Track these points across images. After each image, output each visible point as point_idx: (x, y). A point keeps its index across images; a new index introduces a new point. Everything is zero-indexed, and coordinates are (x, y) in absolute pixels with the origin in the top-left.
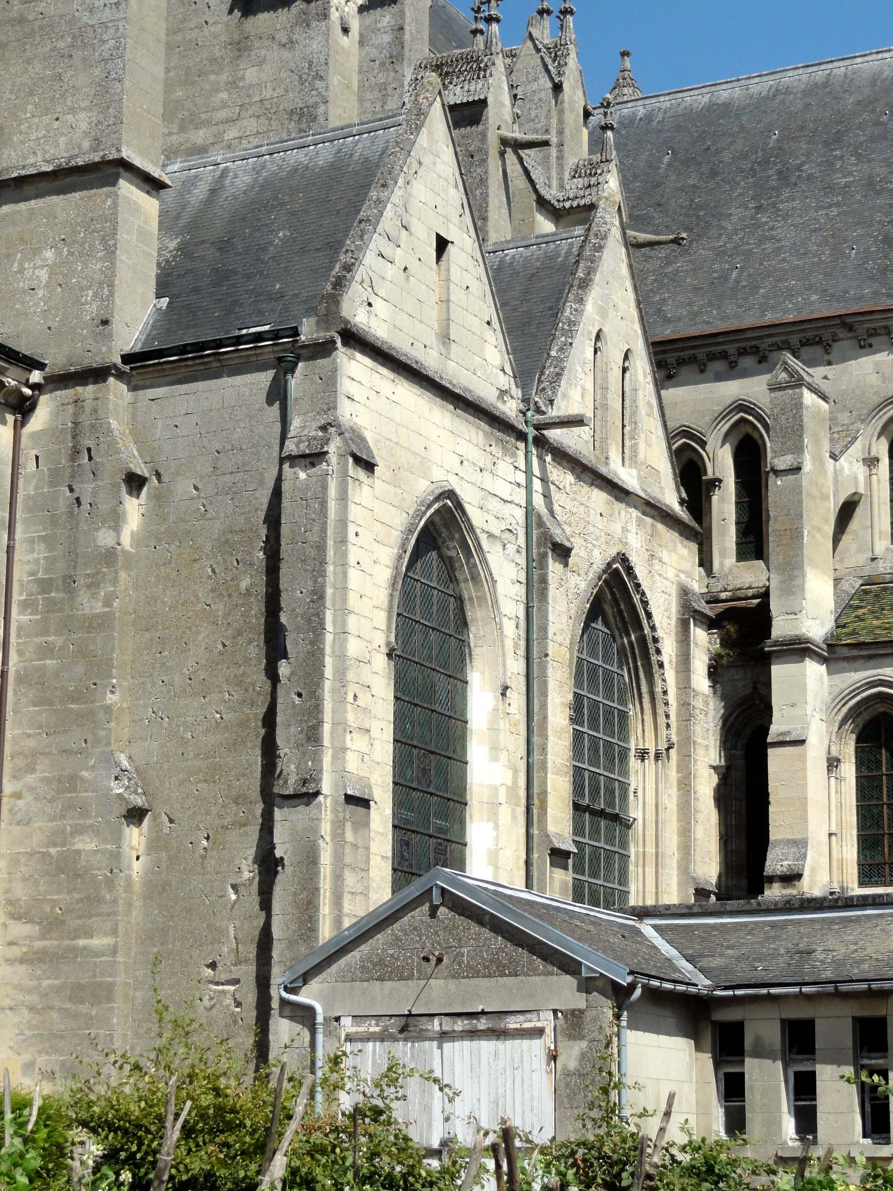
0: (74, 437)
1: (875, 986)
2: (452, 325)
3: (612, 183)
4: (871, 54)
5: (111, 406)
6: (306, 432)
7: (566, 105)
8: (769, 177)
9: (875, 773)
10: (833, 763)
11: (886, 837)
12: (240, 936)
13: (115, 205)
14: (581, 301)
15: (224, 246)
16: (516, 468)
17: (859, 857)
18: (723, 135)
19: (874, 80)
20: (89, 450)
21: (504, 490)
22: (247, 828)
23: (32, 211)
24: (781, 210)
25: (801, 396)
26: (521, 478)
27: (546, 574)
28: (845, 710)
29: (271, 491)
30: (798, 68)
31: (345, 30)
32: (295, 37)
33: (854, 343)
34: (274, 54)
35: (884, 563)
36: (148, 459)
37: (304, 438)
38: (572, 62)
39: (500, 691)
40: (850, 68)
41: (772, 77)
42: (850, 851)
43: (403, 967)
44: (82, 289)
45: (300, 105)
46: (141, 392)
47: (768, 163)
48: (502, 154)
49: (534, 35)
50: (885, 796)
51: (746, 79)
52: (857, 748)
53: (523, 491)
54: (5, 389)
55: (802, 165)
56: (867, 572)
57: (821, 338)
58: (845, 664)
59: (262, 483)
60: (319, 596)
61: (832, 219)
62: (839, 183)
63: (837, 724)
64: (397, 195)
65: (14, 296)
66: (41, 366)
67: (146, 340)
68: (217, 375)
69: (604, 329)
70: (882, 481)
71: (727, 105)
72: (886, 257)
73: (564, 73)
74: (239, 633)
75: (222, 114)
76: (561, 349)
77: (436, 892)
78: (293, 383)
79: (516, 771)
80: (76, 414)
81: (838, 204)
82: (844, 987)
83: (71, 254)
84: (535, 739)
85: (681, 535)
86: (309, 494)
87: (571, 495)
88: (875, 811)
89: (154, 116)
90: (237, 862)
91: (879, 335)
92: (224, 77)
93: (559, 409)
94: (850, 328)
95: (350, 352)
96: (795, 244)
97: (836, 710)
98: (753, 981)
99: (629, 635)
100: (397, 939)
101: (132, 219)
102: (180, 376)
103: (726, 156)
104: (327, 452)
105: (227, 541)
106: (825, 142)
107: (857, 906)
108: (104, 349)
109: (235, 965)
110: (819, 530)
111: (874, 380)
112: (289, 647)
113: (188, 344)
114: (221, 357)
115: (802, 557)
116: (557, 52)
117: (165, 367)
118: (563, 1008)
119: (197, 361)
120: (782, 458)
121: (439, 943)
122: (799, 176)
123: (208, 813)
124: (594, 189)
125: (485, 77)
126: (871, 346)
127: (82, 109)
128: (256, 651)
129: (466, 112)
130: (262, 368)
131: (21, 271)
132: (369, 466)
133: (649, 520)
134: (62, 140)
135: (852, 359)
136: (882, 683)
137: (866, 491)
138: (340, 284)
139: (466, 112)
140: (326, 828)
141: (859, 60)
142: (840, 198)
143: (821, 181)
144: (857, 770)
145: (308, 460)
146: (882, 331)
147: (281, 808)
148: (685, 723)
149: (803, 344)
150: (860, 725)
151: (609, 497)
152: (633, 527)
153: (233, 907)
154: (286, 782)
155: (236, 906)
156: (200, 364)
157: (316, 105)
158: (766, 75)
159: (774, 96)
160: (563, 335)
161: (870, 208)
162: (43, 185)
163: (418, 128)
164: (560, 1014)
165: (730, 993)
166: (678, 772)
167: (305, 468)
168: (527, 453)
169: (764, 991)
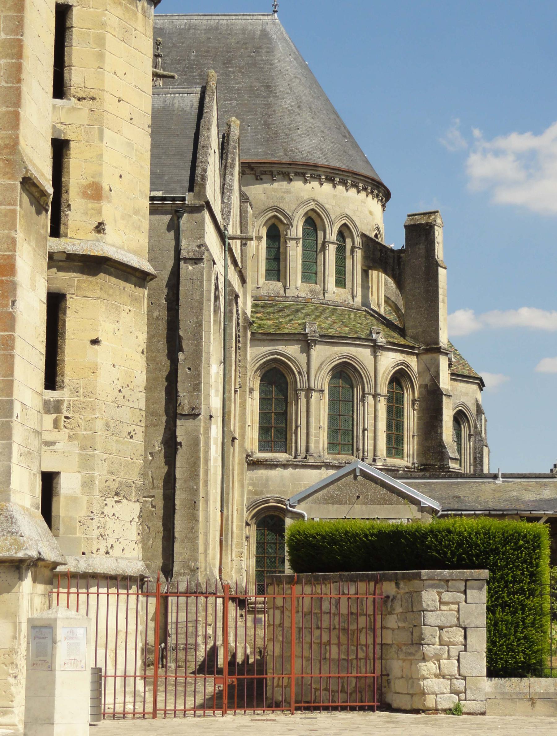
1: (505, 512)
4: (240, 15)
6: (190, 247)
8: (194, 76)
9: (269, 397)
11: (273, 428)
12: (154, 476)
19: (244, 30)
22: (158, 427)
28: (258, 365)
29: (169, 272)
30: (200, 15)
33: (254, 177)
40: (229, 21)
41: (186, 18)
43: (342, 499)
47: (192, 68)
51: (170, 16)
58: (259, 343)
59: (164, 267)
60: (199, 325)
61: (234, 107)
62: (234, 87)
63: (253, 372)
72: (267, 133)
76: (228, 199)
77: (358, 471)
82: (493, 512)
84: (227, 386)
86: (194, 277)
88: (268, 416)
90: (153, 442)
91: (267, 174)
94: (252, 169)
98: (452, 509)
100: (340, 488)
106: (222, 62)
109: (152, 489)
111: (262, 197)
112: (184, 346)
121: (358, 490)
126: (261, 179)
130: (166, 213)
135: (252, 185)
136: (277, 353)
141: (234, 17)
142: (236, 96)
143: (225, 84)
145: (193, 261)
147: (180, 419)
153: (150, 463)
154: (183, 408)
155: (152, 462)
158: (182, 16)
159: (189, 29)
161: (254, 104)
165: (446, 513)
169: (460, 513)
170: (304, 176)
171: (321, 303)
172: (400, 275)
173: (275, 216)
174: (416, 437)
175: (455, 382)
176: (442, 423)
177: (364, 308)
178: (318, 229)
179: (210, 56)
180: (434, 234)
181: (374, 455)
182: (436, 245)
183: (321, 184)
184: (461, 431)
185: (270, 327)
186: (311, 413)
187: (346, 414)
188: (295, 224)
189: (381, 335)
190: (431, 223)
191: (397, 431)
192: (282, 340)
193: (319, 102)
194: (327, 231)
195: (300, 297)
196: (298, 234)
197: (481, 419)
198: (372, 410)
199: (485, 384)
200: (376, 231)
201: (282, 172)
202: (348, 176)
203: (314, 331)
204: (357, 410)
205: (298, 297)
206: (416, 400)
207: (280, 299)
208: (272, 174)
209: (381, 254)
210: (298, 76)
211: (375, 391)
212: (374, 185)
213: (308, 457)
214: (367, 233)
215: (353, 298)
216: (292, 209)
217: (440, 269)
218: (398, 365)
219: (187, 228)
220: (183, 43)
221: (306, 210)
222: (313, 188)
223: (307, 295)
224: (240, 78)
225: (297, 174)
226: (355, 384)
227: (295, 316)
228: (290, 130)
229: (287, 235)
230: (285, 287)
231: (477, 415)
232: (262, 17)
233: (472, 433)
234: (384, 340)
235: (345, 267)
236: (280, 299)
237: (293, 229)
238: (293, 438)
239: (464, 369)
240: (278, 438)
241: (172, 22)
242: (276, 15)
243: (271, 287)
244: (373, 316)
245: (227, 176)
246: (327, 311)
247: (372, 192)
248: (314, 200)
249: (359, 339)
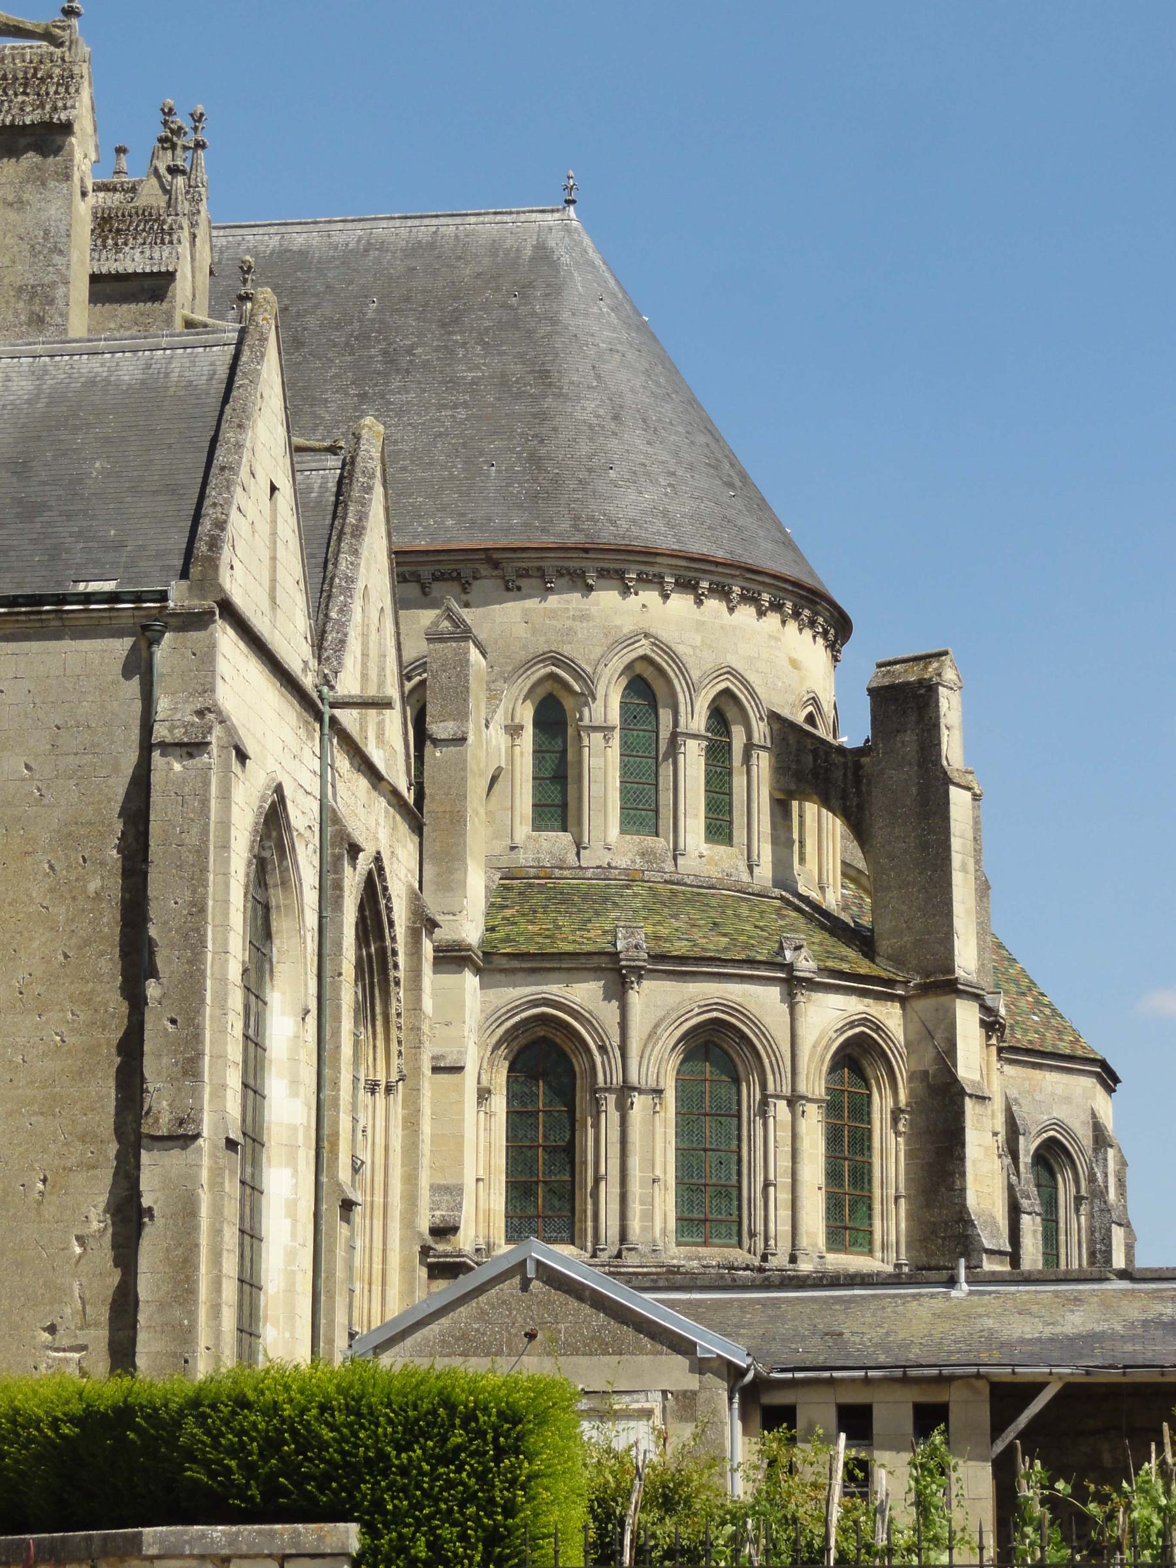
1: (946, 1371)
4: (487, 214)
6: (178, 716)
8: (371, 357)
9: (530, 1108)
10: (484, 1094)
12: (87, 1296)
14: (355, 552)
17: (506, 1208)
18: (304, 292)
19: (494, 247)
22: (97, 1172)
24: (392, 403)
25: (467, 652)
27: (342, 879)
28: (500, 1031)
29: (128, 780)
30: (394, 218)
32: (25, 197)
33: (500, 582)
35: (525, 853)
37: (178, 723)
39: (301, 1016)
40: (461, 228)
41: (361, 225)
42: (498, 1201)
43: (491, 1343)
45: (31, 282)
47: (368, 338)
50: (541, 1135)
51: (325, 222)
52: (508, 1077)
55: (413, 347)
56: (504, 862)
57: (459, 574)
58: (501, 977)
59: (116, 768)
60: (199, 909)
61: (461, 423)
62: (464, 378)
63: (490, 1049)
68: (57, 636)
70: (526, 754)
71: (303, 253)
72: (535, 480)
74: (87, 943)
76: (341, 611)
79: (310, 1108)
81: (465, 405)
82: (913, 1372)
84: (327, 1071)
85: (410, 828)
90: (84, 1209)
91: (529, 576)
94: (496, 565)
96: (415, 449)
97: (489, 1032)
98: (808, 1364)
99: (368, 946)
100: (483, 1312)
102: (7, 632)
103: (312, 322)
104: (209, 743)
105: (70, 834)
106: (439, 321)
107: (844, 1285)
109: (81, 1329)
110: (477, 814)
111: (521, 630)
112: (160, 965)
114: (65, 616)
115: (465, 846)
118: (673, 1389)
119: (32, 617)
120: (441, 725)
121: (532, 1318)
122: (411, 361)
123: (45, 1150)
125: (171, 242)
126: (519, 589)
128: (109, 965)
129: (147, 283)
130: (119, 633)
133: (391, 810)
137: (507, 764)
139: (147, 283)
140: (204, 1175)
141: (473, 219)
142: (467, 397)
143: (441, 372)
144: (508, 1103)
145: (185, 750)
146: (536, 574)
147: (149, 1150)
148: (413, 1051)
149: (435, 579)
150: (515, 1052)
152: (382, 821)
153: (78, 1262)
154: (157, 1121)
155: (83, 1261)
156: (35, 620)
157: (53, 285)
158: (353, 221)
159: (366, 250)
161: (507, 415)
164: (669, 1396)
165: (790, 1375)
166: (403, 1108)
167: (180, 759)
169: (827, 1374)
170: (622, 579)
171: (666, 882)
172: (860, 807)
173: (552, 676)
174: (902, 1201)
175: (1038, 1072)
176: (963, 1165)
177: (777, 892)
178: (660, 705)
179: (411, 309)
180: (937, 706)
181: (794, 1245)
182: (944, 732)
183: (666, 597)
184: (1056, 1188)
185: (531, 939)
186: (630, 1147)
187: (723, 1147)
188: (600, 692)
189: (804, 952)
190: (930, 679)
191: (855, 1188)
192: (559, 969)
193: (668, 406)
194: (682, 708)
195: (616, 868)
196: (609, 717)
197: (1106, 1160)
198: (785, 1135)
199: (1119, 1074)
200: (810, 708)
201: (567, 569)
202: (733, 576)
203: (636, 947)
204: (749, 1136)
205: (610, 866)
206: (902, 1111)
207: (566, 873)
208: (543, 576)
209: (815, 760)
210: (619, 347)
211: (793, 1090)
212: (802, 597)
213: (624, 1253)
214: (786, 713)
215: (750, 868)
216: (592, 657)
217: (953, 790)
218: (852, 1025)
219: (172, 668)
220: (351, 282)
221: (627, 660)
222: (644, 606)
223: (633, 862)
224: (478, 355)
225: (603, 574)
226: (742, 1073)
227: (597, 914)
228: (590, 470)
229: (581, 719)
230: (579, 846)
231: (1095, 1150)
232: (539, 216)
233: (1083, 1193)
234: (812, 965)
235: (730, 794)
236: (566, 873)
237: (597, 707)
238: (589, 1207)
239: (1061, 1040)
240: (552, 1208)
241: (329, 236)
242: (571, 210)
243: (545, 844)
244: (798, 909)
245: (342, 556)
246: (681, 897)
247: (796, 615)
248: (646, 636)
249: (751, 962)
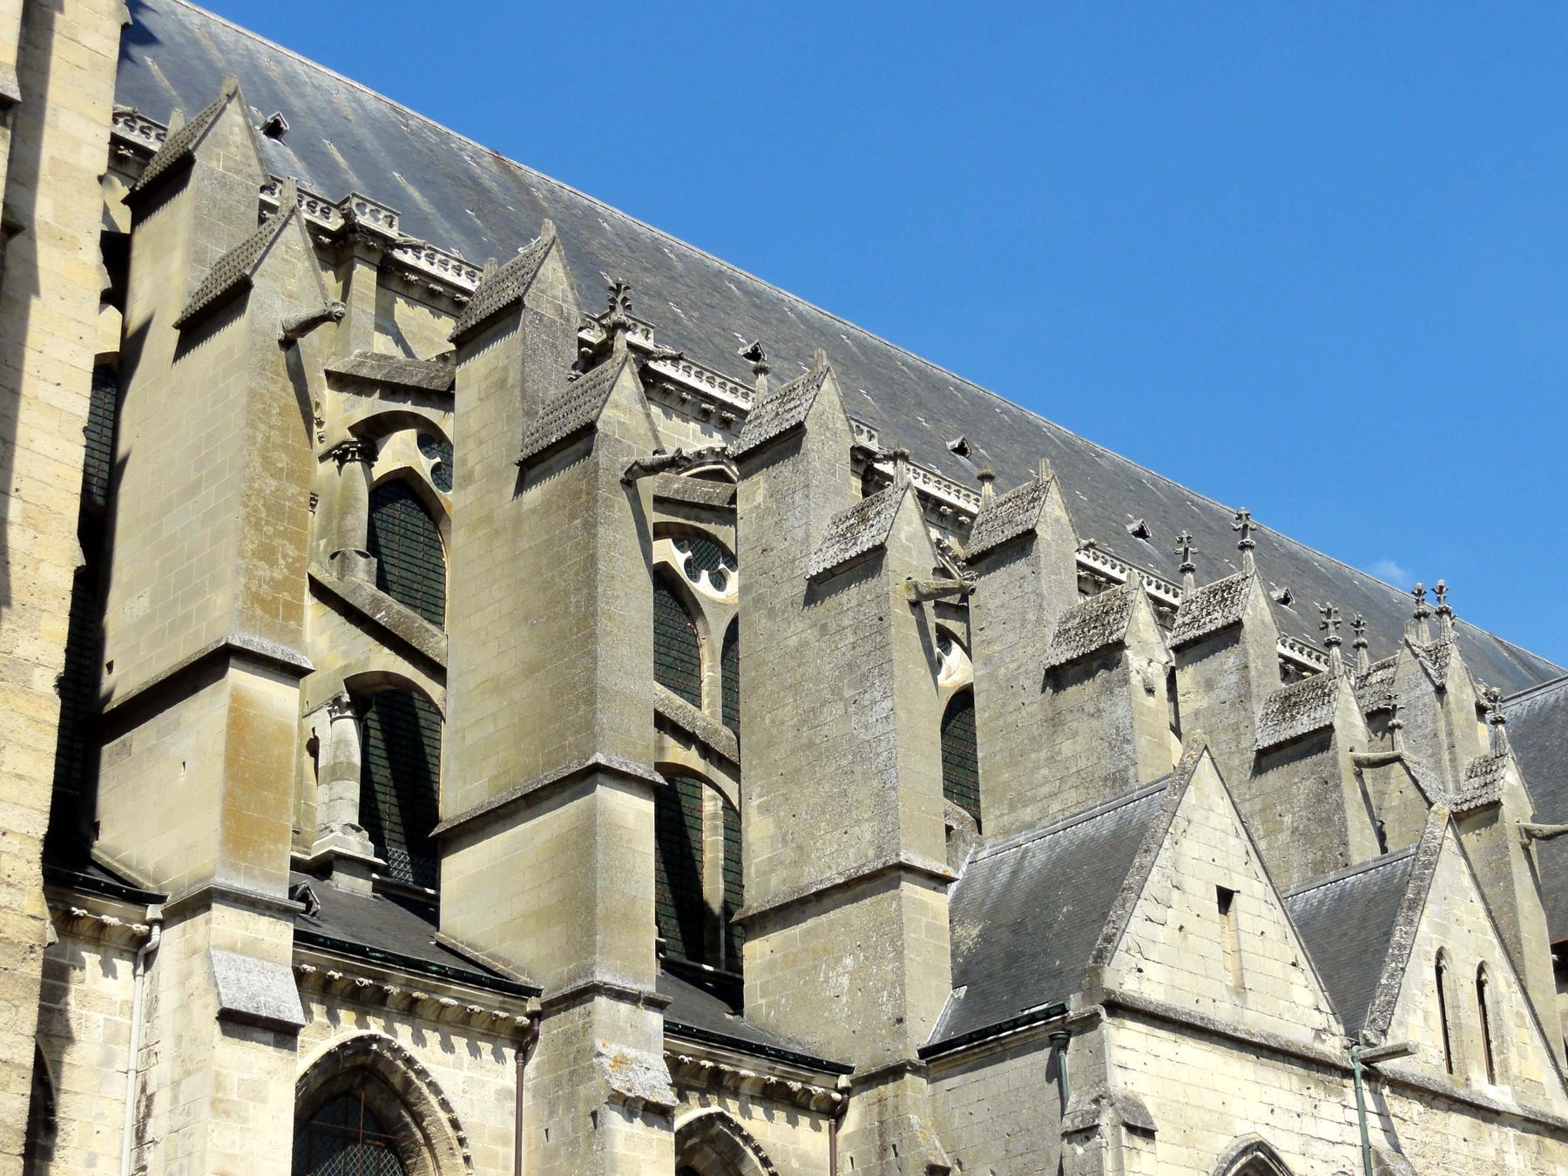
0: (881, 1136)
2: (1247, 976)
3: (1510, 776)
5: (909, 1102)
6: (1080, 1107)
7: (1452, 706)
13: (900, 907)
15: (1016, 928)
16: (1345, 1106)
20: (894, 1146)
21: (1333, 1132)
23: (831, 922)
26: (1354, 1116)
31: (1150, 691)
32: (1102, 706)
34: (1084, 725)
36: (949, 1149)
37: (1079, 1113)
38: (1455, 661)
44: (878, 991)
45: (1112, 771)
46: (939, 1083)
48: (1359, 775)
49: (1410, 641)
53: (1357, 1130)
54: (814, 1098)
64: (1164, 857)
65: (822, 1005)
66: (847, 1070)
67: (944, 1031)
68: (1002, 1060)
69: (1446, 946)
73: (1446, 674)
75: (1045, 790)
76: (1392, 976)
78: (1067, 1059)
80: (881, 1114)
83: (867, 958)
86: (1087, 1168)
87: (1421, 1125)
89: (935, 815)
92: (1043, 754)
93: (1394, 1038)
95: (1117, 1021)
101: (918, 917)
102: (970, 1064)
104: (1098, 1126)
108: (901, 1047)
113: (973, 1033)
116: (1437, 654)
117: (955, 1057)
119: (982, 1048)
124: (1491, 787)
125: (1329, 702)
127: (866, 820)
129: (1315, 739)
130: (1039, 1048)
131: (827, 980)
132: (1148, 1134)
133: (1532, 1137)
134: (851, 852)
138: (1100, 957)
139: (1315, 739)
145: (1083, 1135)
151: (1474, 1120)
152: (1511, 1147)
156: (983, 1051)
157: (1126, 769)
160: (1393, 961)
162: (838, 896)
163: (1183, 789)
167: (1081, 1143)
168: (1357, 1091)
219: (1077, 1067)
